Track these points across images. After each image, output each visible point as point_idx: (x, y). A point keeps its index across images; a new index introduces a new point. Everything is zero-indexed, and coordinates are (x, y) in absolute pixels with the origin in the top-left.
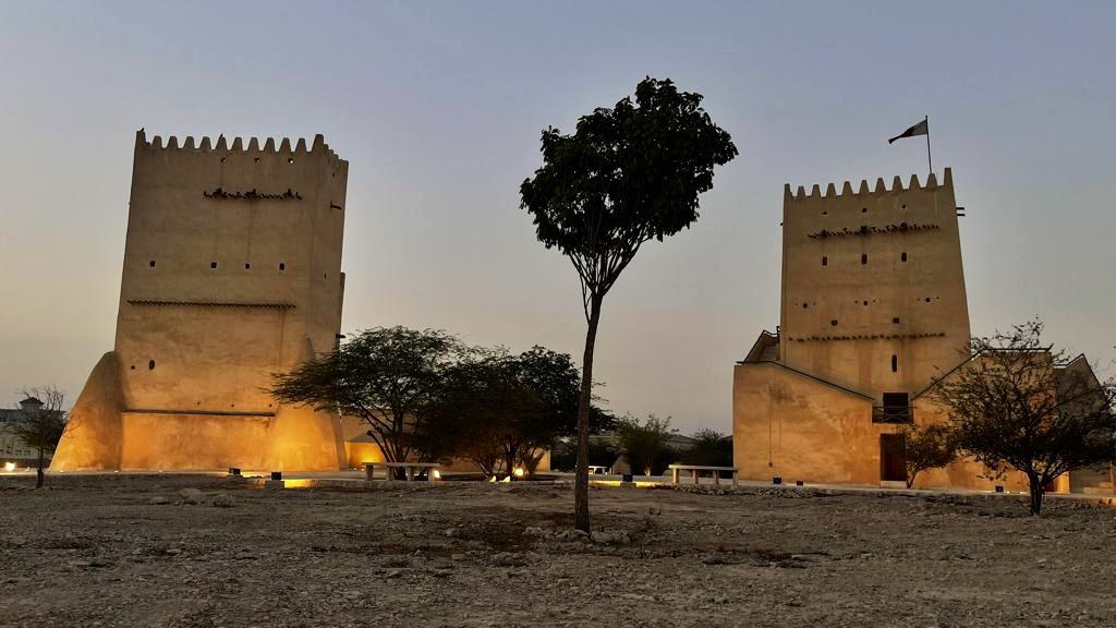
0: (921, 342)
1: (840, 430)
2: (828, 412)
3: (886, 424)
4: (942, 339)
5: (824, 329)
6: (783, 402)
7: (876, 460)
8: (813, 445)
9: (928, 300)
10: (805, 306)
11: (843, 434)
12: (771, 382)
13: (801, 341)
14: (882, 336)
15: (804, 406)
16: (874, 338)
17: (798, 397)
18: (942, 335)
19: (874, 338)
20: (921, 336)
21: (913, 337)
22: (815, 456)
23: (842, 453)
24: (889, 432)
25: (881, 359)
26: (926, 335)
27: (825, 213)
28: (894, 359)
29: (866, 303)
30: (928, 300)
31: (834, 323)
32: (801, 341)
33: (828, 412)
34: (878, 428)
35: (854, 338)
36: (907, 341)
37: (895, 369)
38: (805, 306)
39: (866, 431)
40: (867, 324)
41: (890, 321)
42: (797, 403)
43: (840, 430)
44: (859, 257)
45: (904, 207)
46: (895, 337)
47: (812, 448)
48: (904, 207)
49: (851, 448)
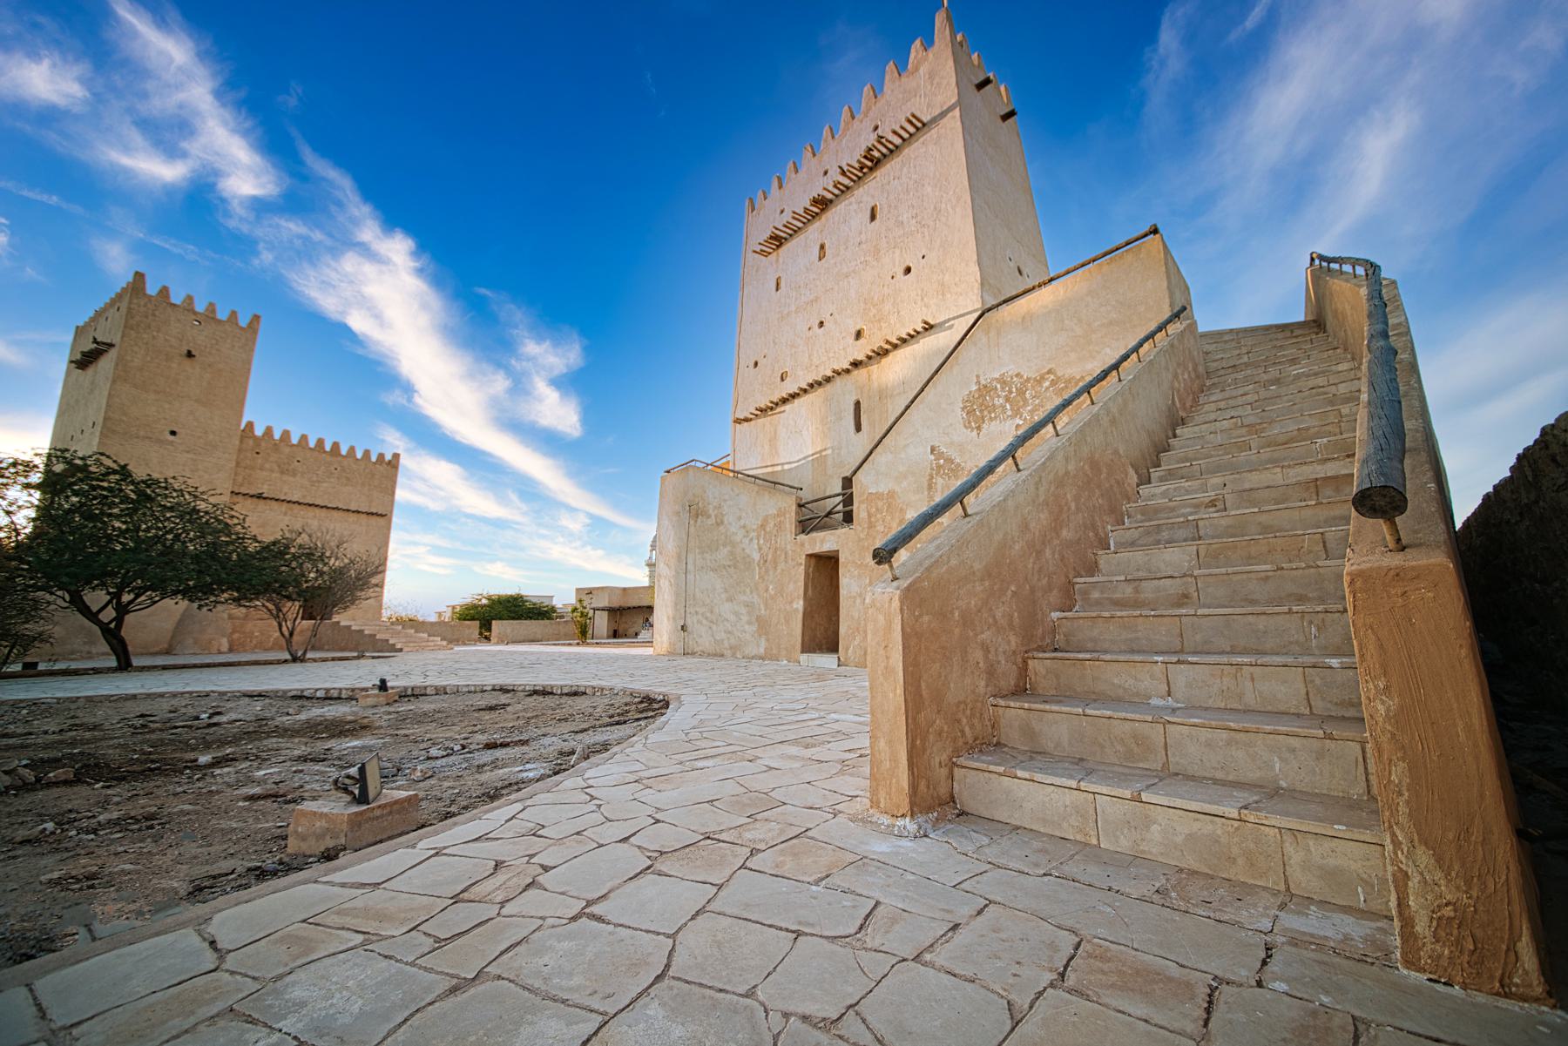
1: (756, 556)
2: (744, 527)
3: (814, 534)
7: (797, 610)
10: (756, 364)
15: (720, 523)
16: (828, 380)
19: (828, 380)
20: (896, 347)
22: (726, 609)
24: (817, 550)
26: (904, 341)
28: (858, 404)
34: (802, 545)
37: (858, 428)
38: (756, 364)
42: (712, 521)
43: (756, 556)
49: (767, 590)
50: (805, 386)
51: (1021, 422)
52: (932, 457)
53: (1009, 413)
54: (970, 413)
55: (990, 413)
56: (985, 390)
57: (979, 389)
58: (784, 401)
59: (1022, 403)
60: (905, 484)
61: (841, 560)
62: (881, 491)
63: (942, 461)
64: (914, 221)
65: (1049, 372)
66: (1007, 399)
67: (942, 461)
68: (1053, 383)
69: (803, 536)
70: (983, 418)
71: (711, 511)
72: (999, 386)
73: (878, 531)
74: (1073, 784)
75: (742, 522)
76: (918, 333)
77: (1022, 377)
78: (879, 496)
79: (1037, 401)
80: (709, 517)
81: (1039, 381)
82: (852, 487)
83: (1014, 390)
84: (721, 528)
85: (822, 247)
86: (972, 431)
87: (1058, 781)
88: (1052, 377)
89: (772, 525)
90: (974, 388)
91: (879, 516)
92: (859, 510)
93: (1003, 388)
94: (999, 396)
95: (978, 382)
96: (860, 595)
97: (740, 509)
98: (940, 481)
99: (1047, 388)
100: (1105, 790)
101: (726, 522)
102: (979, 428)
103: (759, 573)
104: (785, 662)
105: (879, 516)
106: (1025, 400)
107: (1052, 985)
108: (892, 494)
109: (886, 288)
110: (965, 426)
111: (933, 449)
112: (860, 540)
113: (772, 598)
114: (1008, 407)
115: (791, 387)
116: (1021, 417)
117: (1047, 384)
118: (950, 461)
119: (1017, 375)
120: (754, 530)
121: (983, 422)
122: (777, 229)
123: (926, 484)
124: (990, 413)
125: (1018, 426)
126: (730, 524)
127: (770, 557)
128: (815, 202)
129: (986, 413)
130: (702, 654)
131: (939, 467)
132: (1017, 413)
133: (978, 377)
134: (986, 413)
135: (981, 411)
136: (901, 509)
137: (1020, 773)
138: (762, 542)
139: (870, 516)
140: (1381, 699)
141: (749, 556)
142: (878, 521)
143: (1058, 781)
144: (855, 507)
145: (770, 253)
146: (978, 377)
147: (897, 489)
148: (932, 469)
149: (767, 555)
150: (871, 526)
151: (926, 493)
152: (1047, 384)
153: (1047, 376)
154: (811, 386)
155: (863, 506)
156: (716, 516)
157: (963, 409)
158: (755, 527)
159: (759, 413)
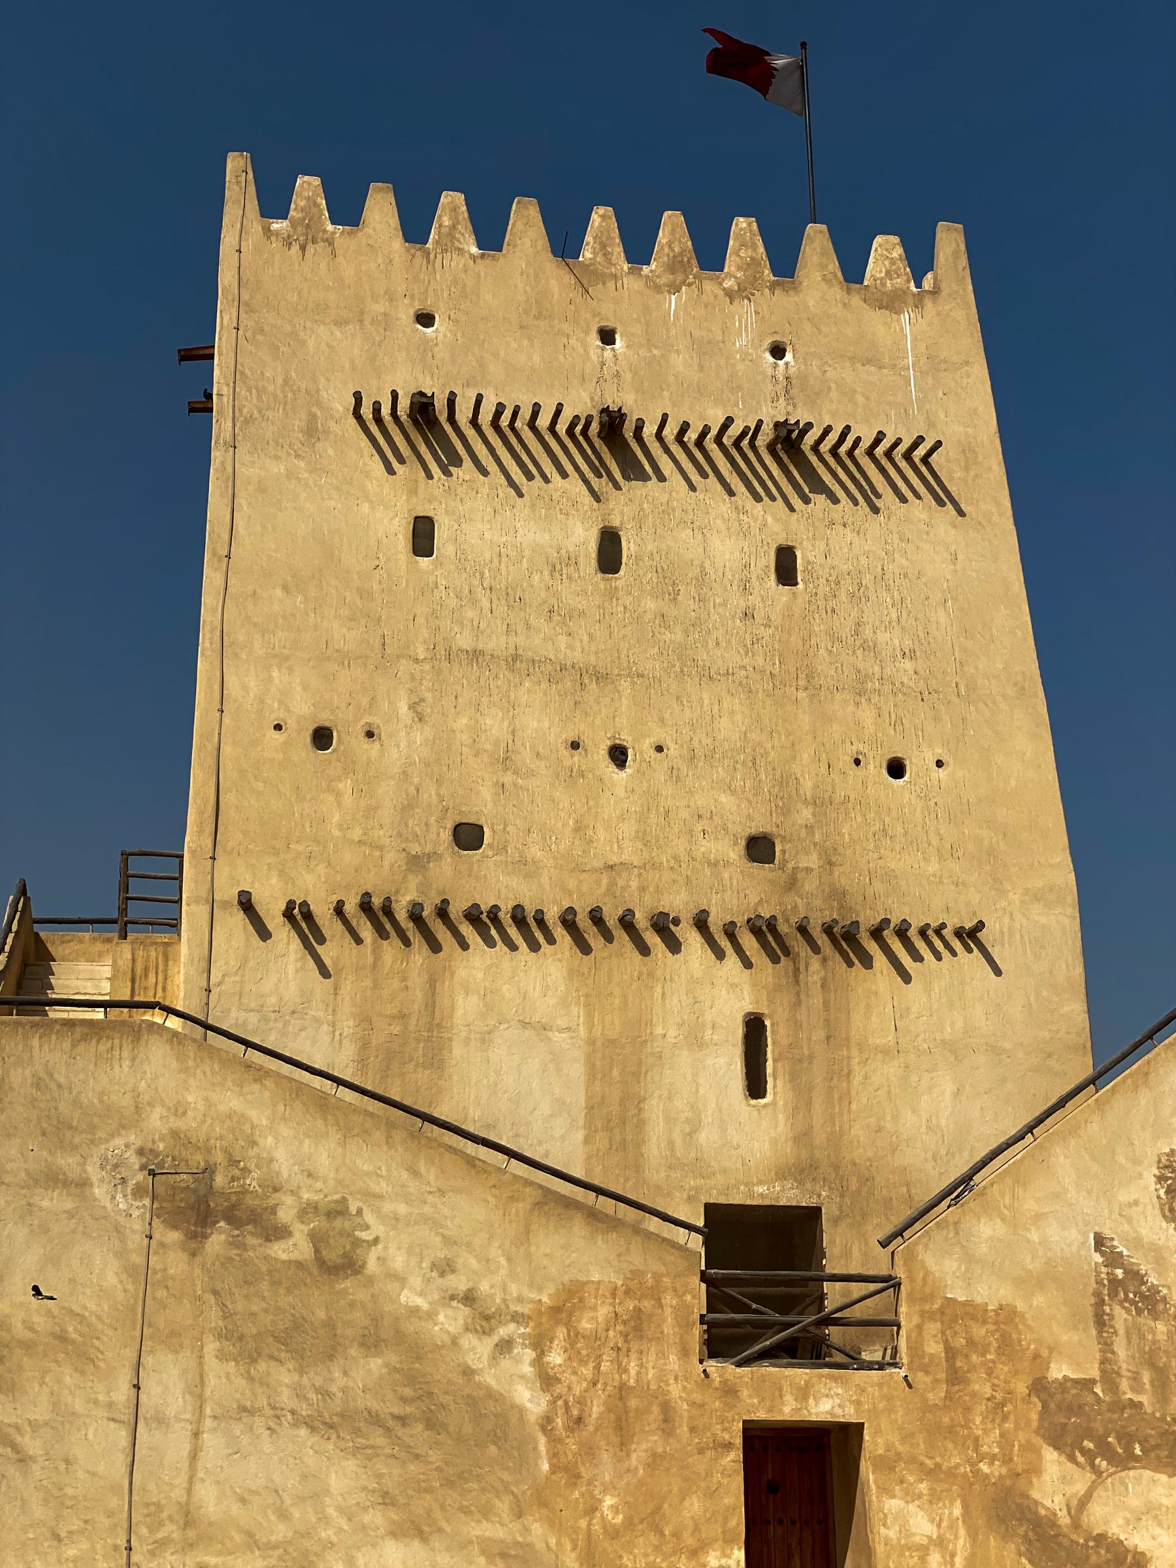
2: (469, 1298)
3: (768, 1370)
5: (417, 863)
6: (217, 1240)
8: (386, 1500)
9: (896, 769)
10: (322, 738)
11: (546, 1423)
12: (156, 1121)
16: (664, 926)
17: (307, 1211)
23: (537, 1530)
24: (788, 1411)
25: (695, 1040)
27: (425, 319)
28: (754, 1029)
30: (896, 769)
33: (469, 1298)
34: (729, 1391)
37: (755, 1086)
38: (322, 738)
39: (667, 1410)
40: (630, 853)
41: (735, 853)
44: (585, 539)
45: (778, 351)
47: (375, 1518)
48: (778, 351)
49: (592, 1510)
52: (1098, 1258)
60: (1039, 1300)
61: (873, 1444)
62: (978, 1300)
63: (1119, 1272)
67: (1119, 1272)
71: (286, 1215)
73: (974, 1395)
75: (459, 1282)
78: (972, 1312)
80: (280, 1233)
84: (347, 1284)
89: (603, 1312)
91: (974, 1358)
96: (941, 1543)
97: (447, 1241)
98: (1121, 1316)
101: (372, 1266)
103: (554, 1455)
105: (974, 1358)
108: (1007, 1316)
109: (835, 776)
110: (1164, 1216)
111: (1100, 1241)
112: (927, 1408)
113: (613, 1533)
118: (1135, 1276)
120: (516, 1318)
123: (1090, 1312)
126: (400, 1279)
127: (596, 1410)
131: (1114, 1282)
136: (1036, 1356)
138: (555, 1358)
139: (951, 1353)
141: (491, 1394)
142: (973, 1368)
147: (1021, 1306)
148: (1099, 1282)
149: (581, 1402)
150: (955, 1378)
151: (1094, 1332)
155: (932, 1328)
156: (316, 1239)
157: (1160, 1179)
158: (525, 1309)
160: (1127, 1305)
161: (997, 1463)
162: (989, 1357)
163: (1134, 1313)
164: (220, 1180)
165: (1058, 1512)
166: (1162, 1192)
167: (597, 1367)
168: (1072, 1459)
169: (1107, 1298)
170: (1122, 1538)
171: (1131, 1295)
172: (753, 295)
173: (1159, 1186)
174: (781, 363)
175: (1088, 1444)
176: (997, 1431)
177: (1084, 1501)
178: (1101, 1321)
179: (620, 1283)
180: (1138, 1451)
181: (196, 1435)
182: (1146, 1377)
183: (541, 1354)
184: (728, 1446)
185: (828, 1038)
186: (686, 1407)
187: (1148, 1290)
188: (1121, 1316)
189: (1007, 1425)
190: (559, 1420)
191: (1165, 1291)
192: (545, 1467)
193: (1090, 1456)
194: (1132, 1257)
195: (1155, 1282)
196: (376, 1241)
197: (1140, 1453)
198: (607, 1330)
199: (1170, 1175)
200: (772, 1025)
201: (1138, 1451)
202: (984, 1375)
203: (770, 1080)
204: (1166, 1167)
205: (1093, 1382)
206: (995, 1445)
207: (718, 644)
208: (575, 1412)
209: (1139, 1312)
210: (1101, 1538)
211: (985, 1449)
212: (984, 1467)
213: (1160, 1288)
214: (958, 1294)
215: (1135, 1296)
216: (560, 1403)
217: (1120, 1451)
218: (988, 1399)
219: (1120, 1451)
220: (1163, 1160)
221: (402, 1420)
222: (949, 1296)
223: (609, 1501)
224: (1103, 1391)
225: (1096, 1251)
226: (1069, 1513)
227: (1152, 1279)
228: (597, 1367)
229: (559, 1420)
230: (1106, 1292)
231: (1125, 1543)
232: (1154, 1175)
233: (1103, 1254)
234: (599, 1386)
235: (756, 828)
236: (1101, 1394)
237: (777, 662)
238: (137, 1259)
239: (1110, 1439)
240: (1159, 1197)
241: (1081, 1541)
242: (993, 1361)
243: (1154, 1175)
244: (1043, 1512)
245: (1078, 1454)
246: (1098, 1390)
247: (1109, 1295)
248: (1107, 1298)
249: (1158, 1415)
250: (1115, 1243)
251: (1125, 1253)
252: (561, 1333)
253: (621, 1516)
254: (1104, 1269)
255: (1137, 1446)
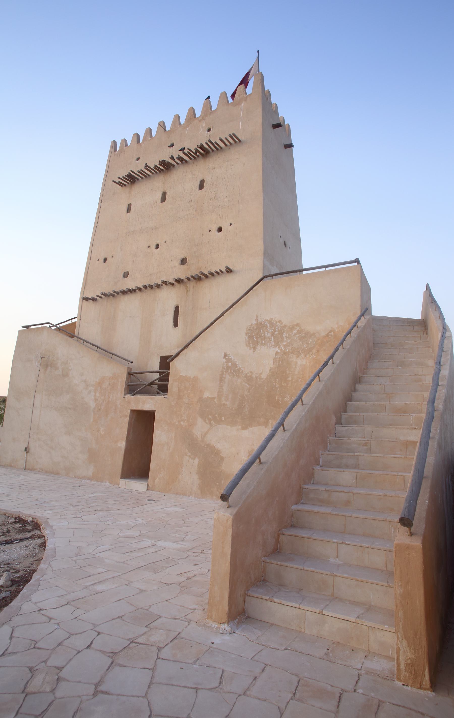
0: (206, 285)
1: (92, 405)
3: (138, 397)
4: (230, 277)
10: (105, 260)
13: (94, 299)
14: (165, 283)
15: (65, 375)
16: (158, 286)
18: (229, 271)
19: (158, 286)
21: (198, 279)
26: (212, 274)
28: (177, 309)
29: (157, 246)
31: (126, 275)
32: (94, 299)
34: (129, 402)
35: (140, 289)
36: (192, 284)
37: (176, 324)
38: (105, 260)
41: (177, 263)
43: (92, 405)
45: (209, 130)
46: (179, 281)
50: (141, 286)
51: (279, 351)
52: (224, 360)
53: (273, 343)
54: (250, 337)
55: (262, 340)
56: (260, 326)
57: (257, 324)
58: (124, 293)
59: (280, 339)
63: (230, 364)
64: (227, 199)
65: (297, 325)
66: (273, 335)
67: (230, 364)
68: (299, 332)
69: (129, 397)
70: (257, 343)
72: (268, 325)
74: (297, 606)
76: (222, 272)
77: (282, 323)
79: (289, 341)
81: (292, 328)
82: (169, 369)
83: (277, 330)
85: (164, 194)
86: (250, 349)
87: (291, 604)
88: (298, 328)
90: (254, 322)
92: (172, 384)
93: (271, 327)
94: (268, 331)
95: (257, 320)
98: (227, 377)
99: (295, 334)
100: (309, 609)
102: (254, 348)
104: (108, 484)
106: (282, 338)
107: (292, 699)
110: (246, 345)
111: (225, 355)
114: (273, 340)
115: (130, 284)
116: (279, 348)
117: (295, 332)
118: (235, 365)
119: (280, 322)
121: (257, 345)
122: (133, 172)
124: (262, 340)
125: (277, 353)
128: (163, 163)
129: (259, 340)
130: (41, 471)
131: (228, 367)
132: (277, 344)
133: (257, 316)
134: (259, 340)
135: (257, 338)
137: (276, 600)
138: (98, 395)
139: (179, 391)
140: (399, 589)
143: (291, 604)
144: (170, 383)
145: (125, 185)
146: (257, 316)
148: (223, 368)
152: (295, 332)
153: (296, 327)
154: (145, 287)
157: (247, 334)
159: (103, 296)
160: (230, 374)
161: (186, 422)
162: (189, 391)
163: (232, 376)
164: (50, 358)
165: (199, 437)
166: (247, 338)
167: (105, 397)
168: (205, 421)
169: (225, 372)
170: (214, 445)
171: (232, 371)
172: (205, 118)
173: (246, 336)
174: (209, 132)
175: (210, 417)
176: (187, 413)
177: (206, 434)
178: (221, 379)
179: (111, 376)
180: (223, 419)
181: (40, 411)
182: (230, 396)
183: (95, 394)
184: (126, 416)
185: (193, 308)
186: (120, 406)
187: (238, 369)
188: (227, 377)
189: (190, 411)
190: (96, 409)
191: (243, 369)
192: (92, 420)
193: (210, 420)
194: (235, 359)
195: (240, 367)
196: (72, 369)
197: (224, 420)
198: (107, 388)
199: (250, 332)
200: (180, 307)
201: (223, 419)
202: (187, 397)
203: (178, 322)
204: (249, 330)
205: (214, 398)
206: (186, 417)
207: (182, 211)
208: (99, 407)
209: (234, 376)
210: (208, 445)
211: (183, 418)
212: (182, 423)
213: (242, 368)
214: (183, 374)
215: (233, 371)
216: (97, 405)
217: (218, 419)
218: (187, 404)
219: (218, 419)
220: (248, 327)
221: (70, 408)
222: (181, 375)
223: (102, 429)
224: (217, 401)
225: (224, 358)
226: (201, 437)
227: (240, 366)
228: (105, 397)
229: (96, 409)
230: (225, 370)
231: (215, 447)
232: (245, 333)
233: (226, 359)
234: (105, 401)
235: (183, 257)
236: (216, 402)
237: (195, 211)
238: (37, 375)
239: (216, 415)
240: (246, 340)
241: (203, 445)
242: (190, 393)
243: (245, 333)
244: (195, 436)
245: (207, 420)
246: (216, 400)
247: (226, 372)
248: (225, 372)
249: (230, 408)
250: (230, 355)
251: (233, 358)
252: (99, 388)
253: (104, 433)
254: (225, 364)
255: (223, 417)
